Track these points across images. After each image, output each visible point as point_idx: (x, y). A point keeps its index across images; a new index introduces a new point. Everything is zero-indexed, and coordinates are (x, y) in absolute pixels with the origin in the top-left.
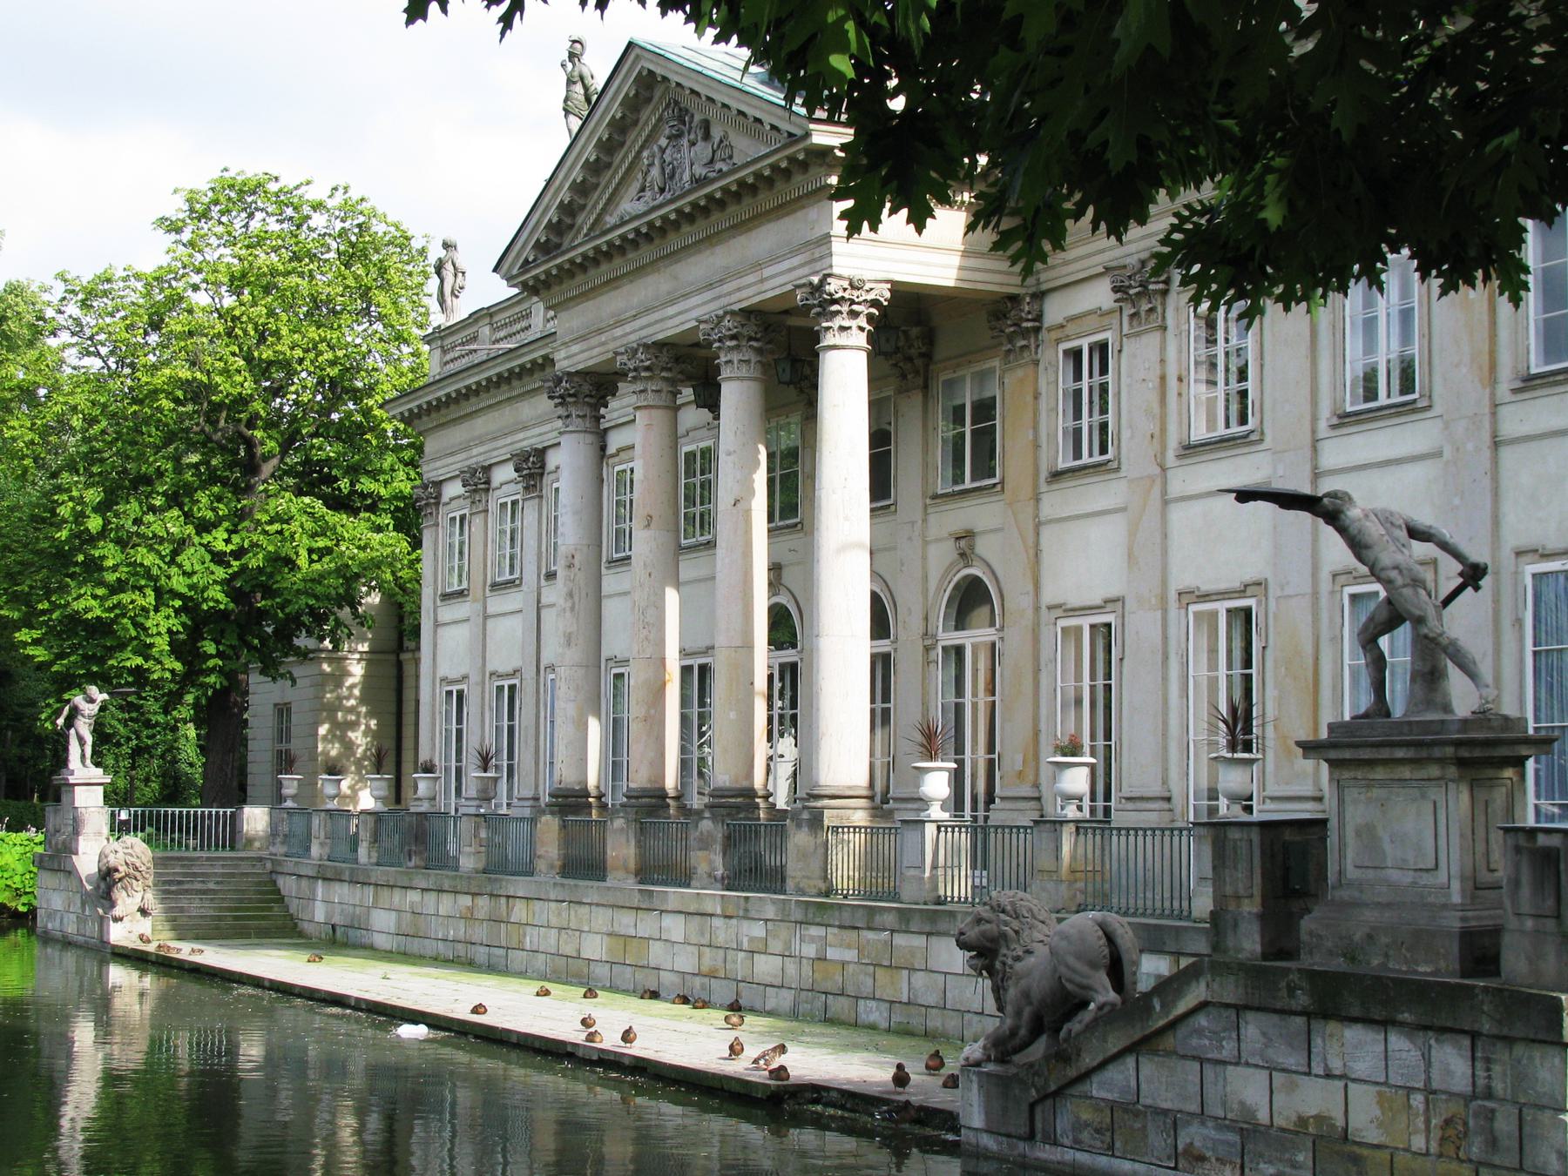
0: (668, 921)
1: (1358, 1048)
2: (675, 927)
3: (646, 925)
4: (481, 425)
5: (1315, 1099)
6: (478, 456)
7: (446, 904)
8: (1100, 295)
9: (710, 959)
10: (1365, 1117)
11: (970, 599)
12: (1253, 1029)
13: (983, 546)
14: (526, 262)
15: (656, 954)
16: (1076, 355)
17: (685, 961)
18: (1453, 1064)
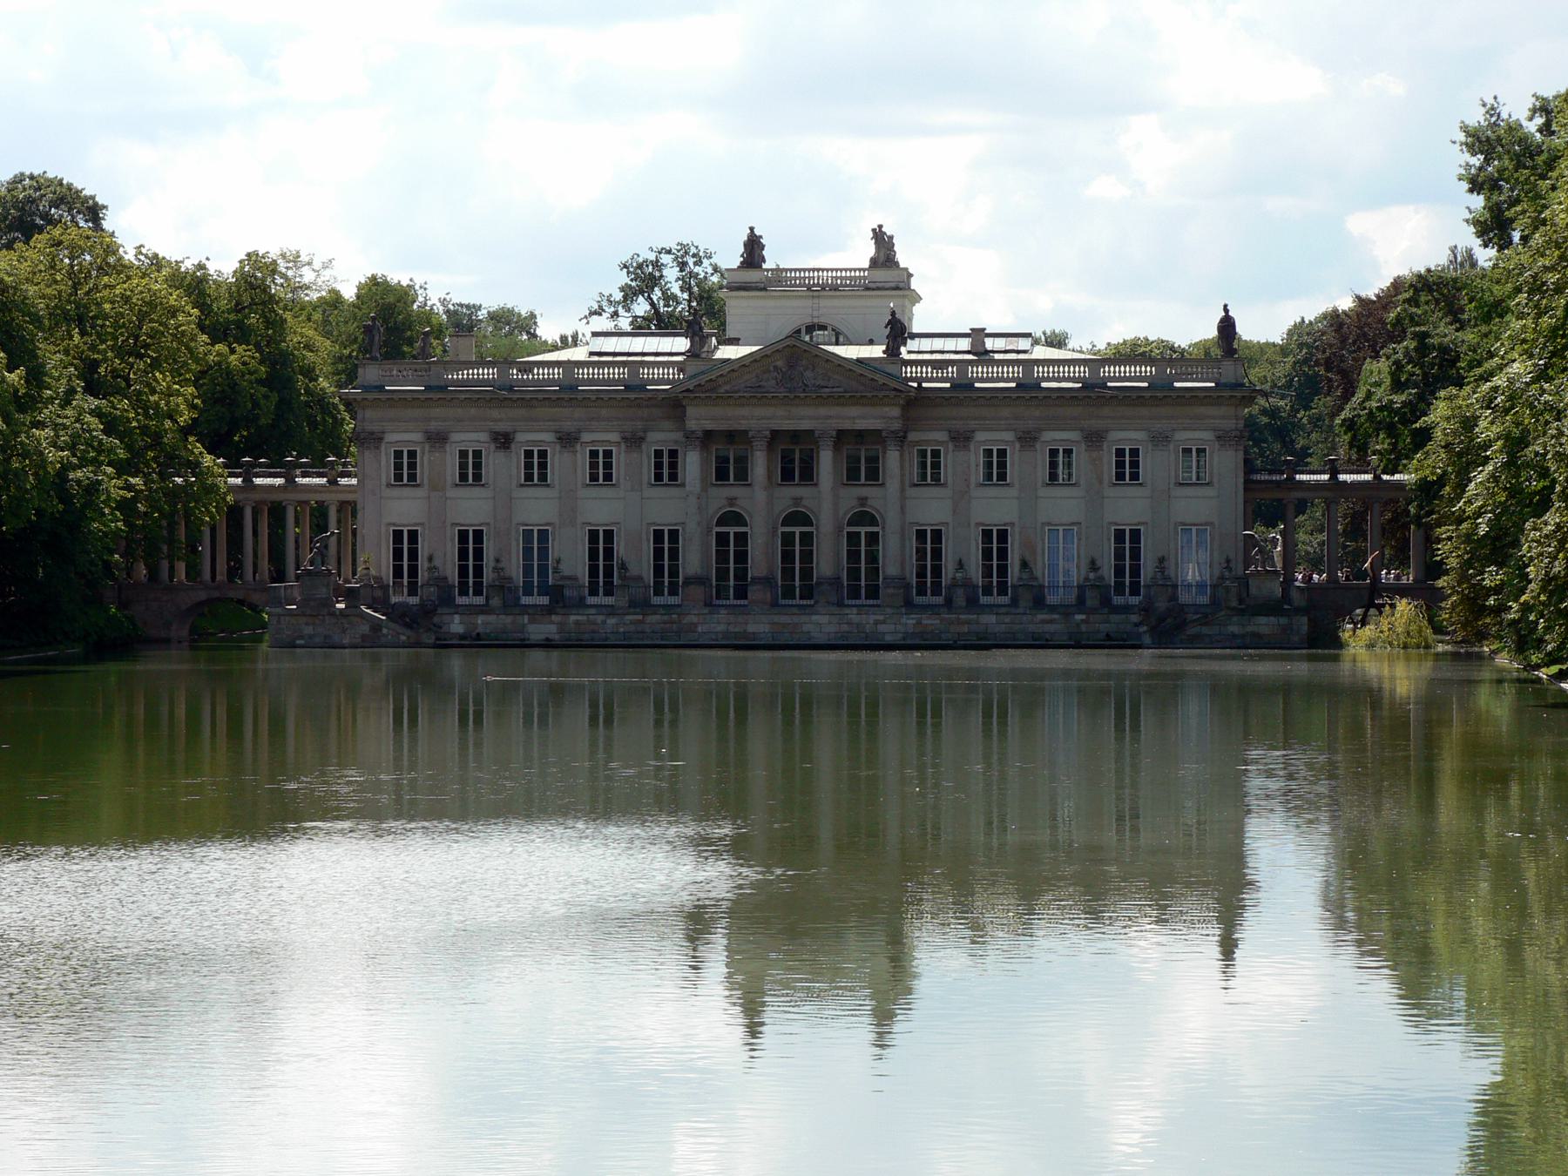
0: (814, 618)
1: (1263, 620)
2: (824, 619)
3: (796, 619)
4: (437, 412)
5: (1250, 629)
6: (434, 426)
7: (612, 621)
8: (942, 436)
9: (845, 628)
10: (1265, 630)
11: (864, 517)
12: (1235, 619)
13: (869, 502)
14: (688, 390)
15: (805, 628)
16: (923, 454)
17: (832, 629)
18: (1283, 621)
